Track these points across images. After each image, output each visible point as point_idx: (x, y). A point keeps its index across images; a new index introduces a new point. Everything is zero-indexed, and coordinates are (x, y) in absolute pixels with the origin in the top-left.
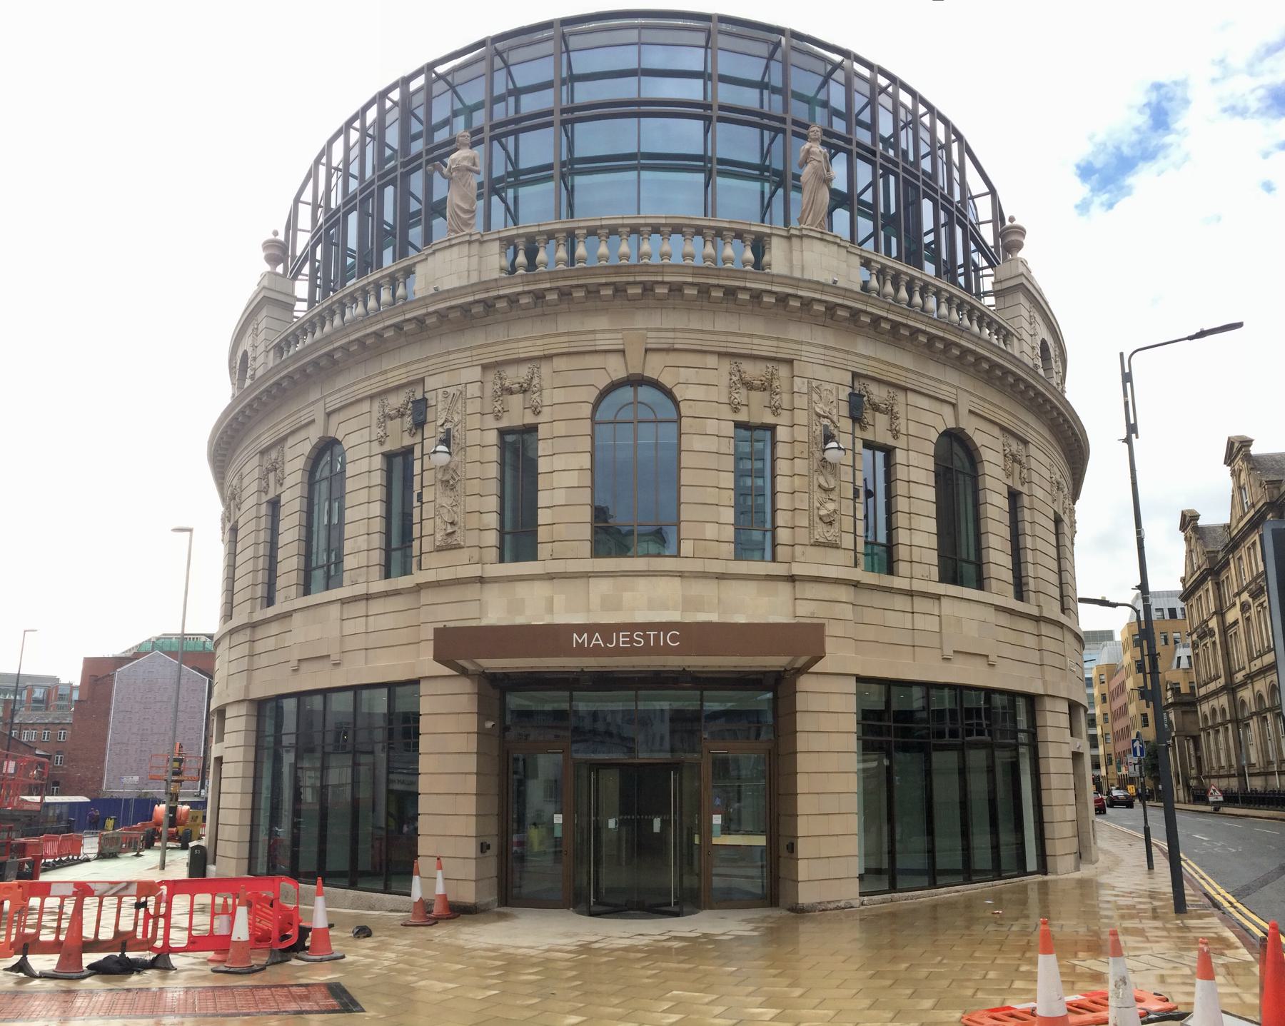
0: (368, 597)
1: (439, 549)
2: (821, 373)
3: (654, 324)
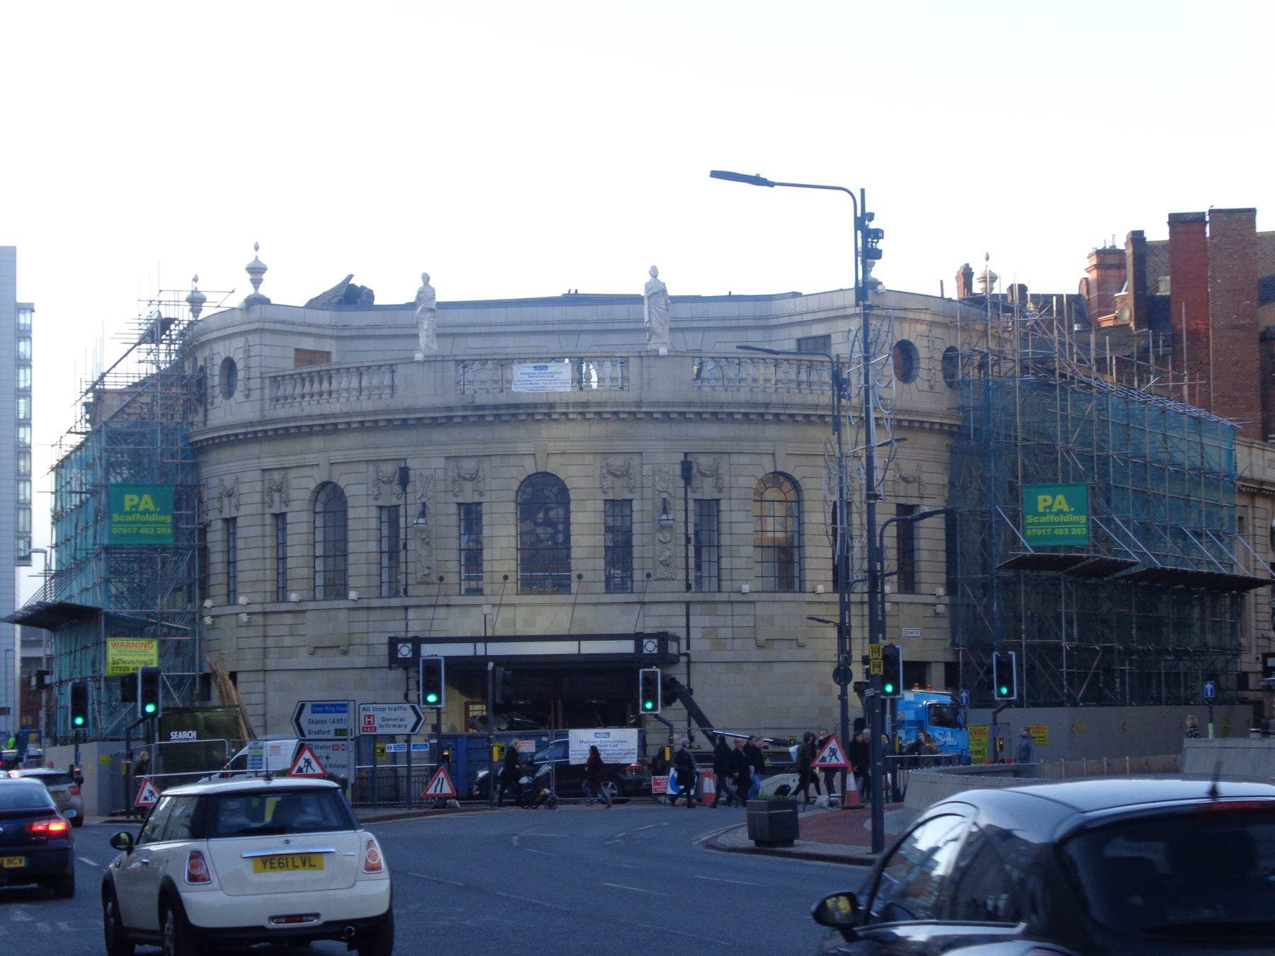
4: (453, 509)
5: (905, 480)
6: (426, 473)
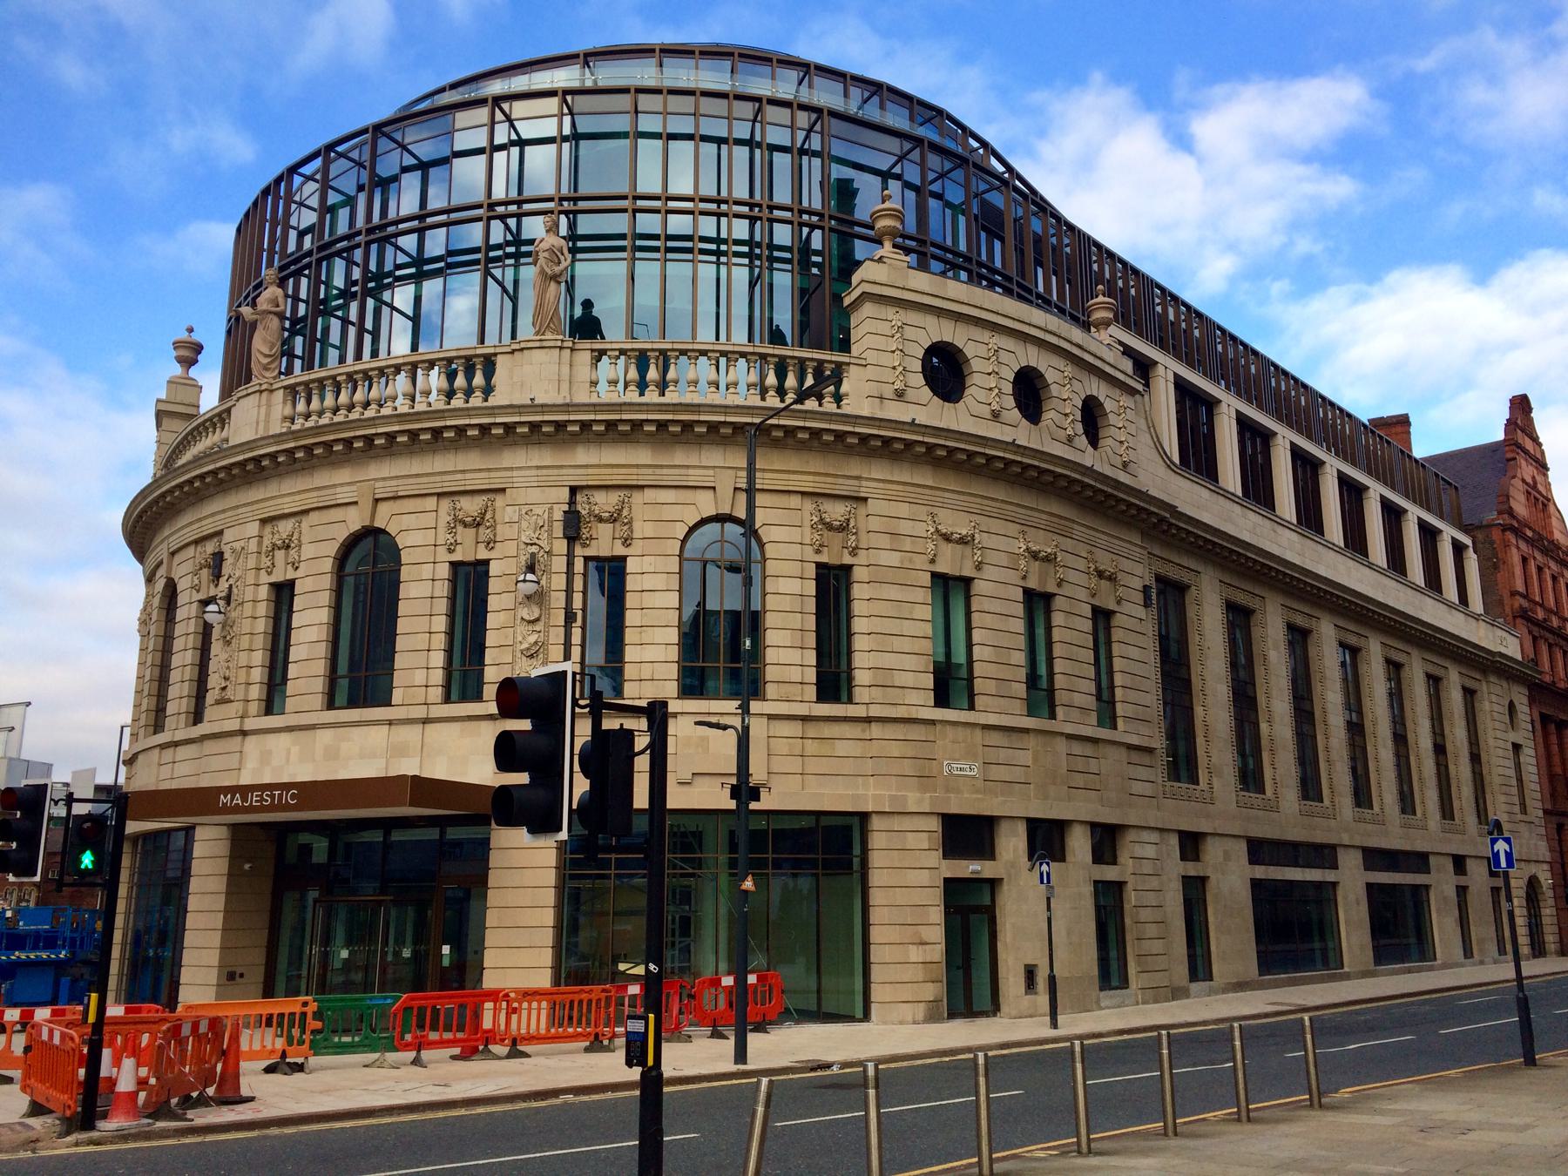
0: (176, 744)
1: (218, 702)
2: (535, 495)
3: (384, 473)
4: (264, 592)
5: (947, 538)
6: (237, 545)
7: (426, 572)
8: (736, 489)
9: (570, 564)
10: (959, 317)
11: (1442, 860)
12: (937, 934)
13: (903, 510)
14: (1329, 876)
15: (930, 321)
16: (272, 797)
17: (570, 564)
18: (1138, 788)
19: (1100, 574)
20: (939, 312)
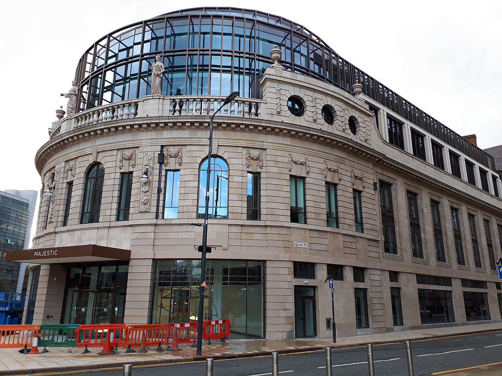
2: (149, 149)
3: (101, 143)
5: (295, 163)
7: (112, 176)
8: (219, 146)
9: (160, 172)
10: (301, 87)
11: (490, 283)
12: (291, 306)
13: (280, 153)
14: (448, 288)
15: (291, 88)
16: (50, 252)
17: (160, 172)
18: (372, 254)
19: (356, 178)
20: (294, 85)
